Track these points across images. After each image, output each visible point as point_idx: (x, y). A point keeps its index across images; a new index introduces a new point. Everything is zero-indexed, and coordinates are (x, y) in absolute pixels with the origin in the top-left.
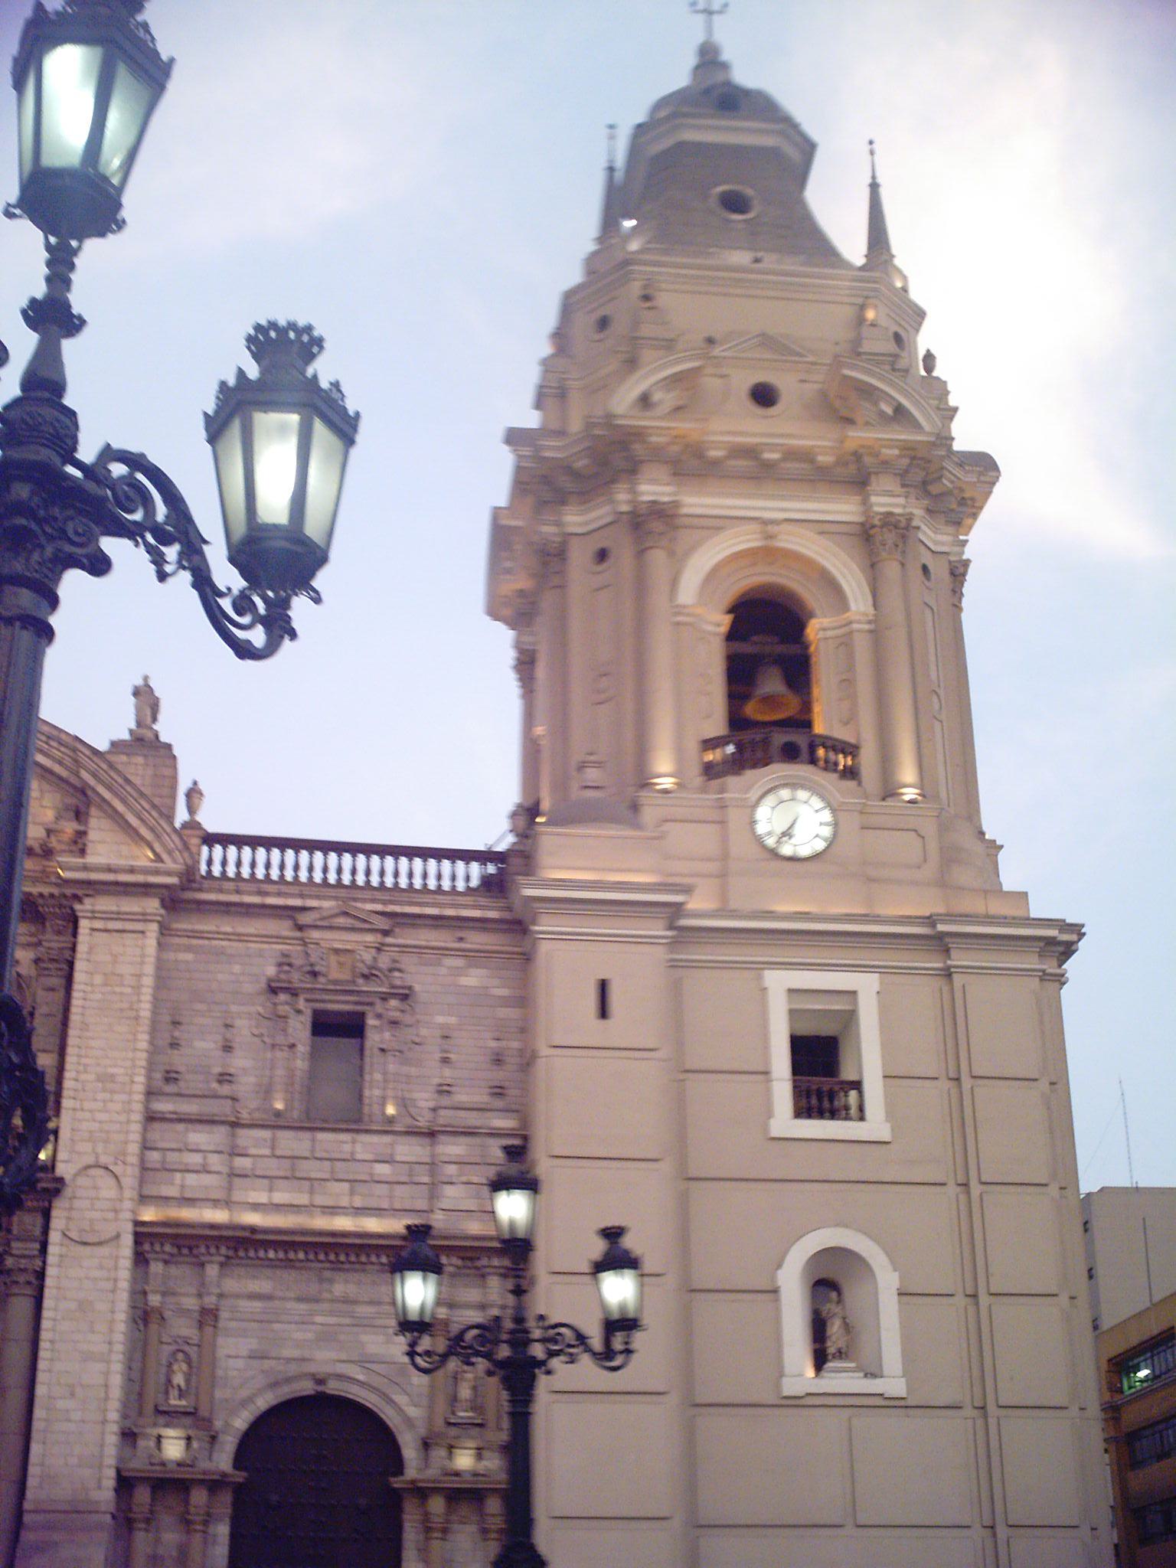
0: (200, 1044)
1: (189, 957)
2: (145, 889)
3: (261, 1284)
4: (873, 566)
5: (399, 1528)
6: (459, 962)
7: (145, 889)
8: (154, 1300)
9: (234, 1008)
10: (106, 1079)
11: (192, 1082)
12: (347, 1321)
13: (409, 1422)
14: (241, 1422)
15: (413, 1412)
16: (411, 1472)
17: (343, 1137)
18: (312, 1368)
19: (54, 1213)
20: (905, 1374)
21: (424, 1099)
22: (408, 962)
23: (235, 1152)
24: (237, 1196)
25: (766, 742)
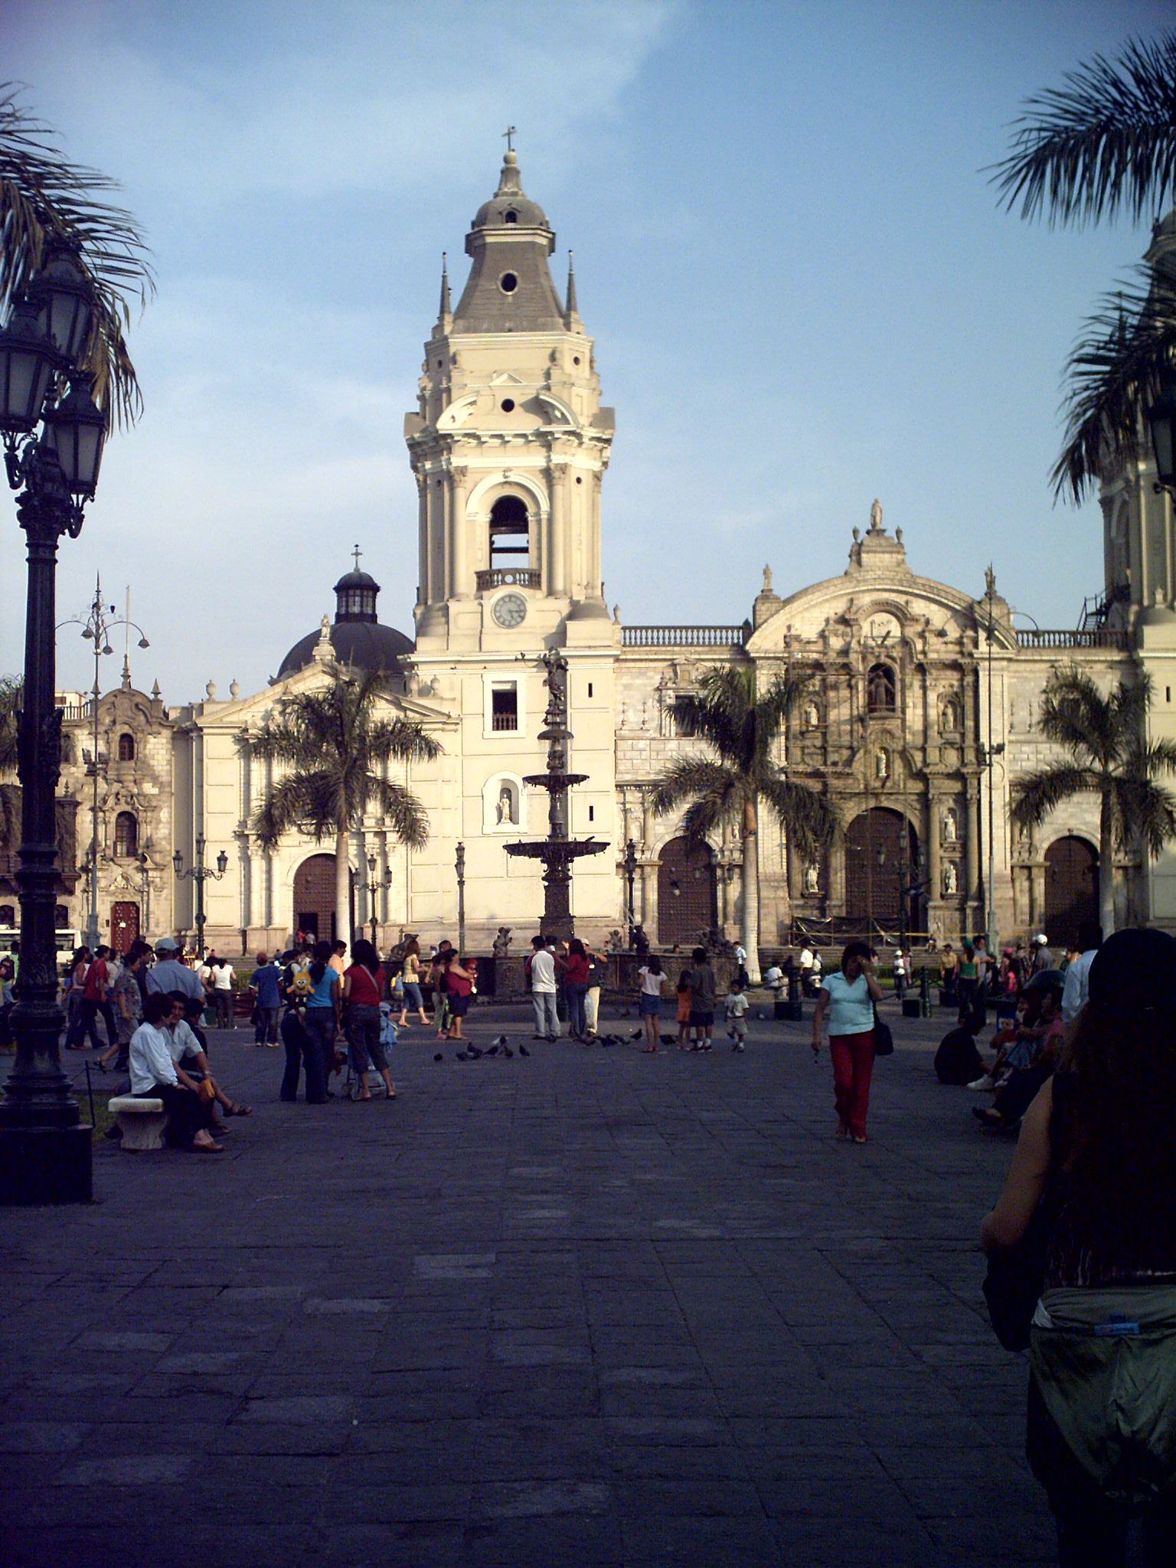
0: (1021, 713)
1: (1015, 680)
7: (1003, 659)
14: (1046, 845)
18: (1068, 827)
19: (982, 779)
23: (1037, 752)
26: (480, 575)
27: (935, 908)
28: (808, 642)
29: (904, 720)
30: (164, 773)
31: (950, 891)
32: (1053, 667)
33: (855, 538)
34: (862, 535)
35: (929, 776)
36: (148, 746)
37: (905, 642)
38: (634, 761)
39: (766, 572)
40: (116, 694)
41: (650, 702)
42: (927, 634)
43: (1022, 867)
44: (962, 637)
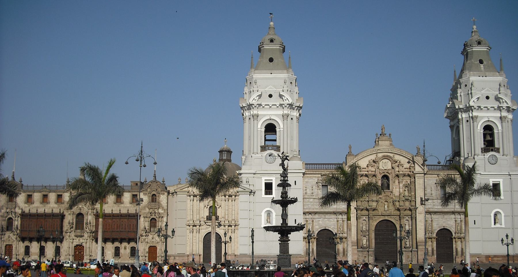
3: (437, 217)
4: (502, 123)
5: (453, 242)
9: (432, 186)
13: (453, 230)
16: (454, 236)
18: (443, 226)
19: (417, 211)
20: (505, 224)
25: (489, 149)
26: (262, 147)
30: (165, 206)
31: (407, 246)
32: (438, 176)
33: (377, 137)
34: (379, 136)
35: (401, 210)
36: (161, 198)
37: (393, 168)
38: (309, 205)
39: (350, 147)
40: (152, 182)
41: (314, 187)
42: (399, 166)
43: (429, 238)
44: (410, 167)
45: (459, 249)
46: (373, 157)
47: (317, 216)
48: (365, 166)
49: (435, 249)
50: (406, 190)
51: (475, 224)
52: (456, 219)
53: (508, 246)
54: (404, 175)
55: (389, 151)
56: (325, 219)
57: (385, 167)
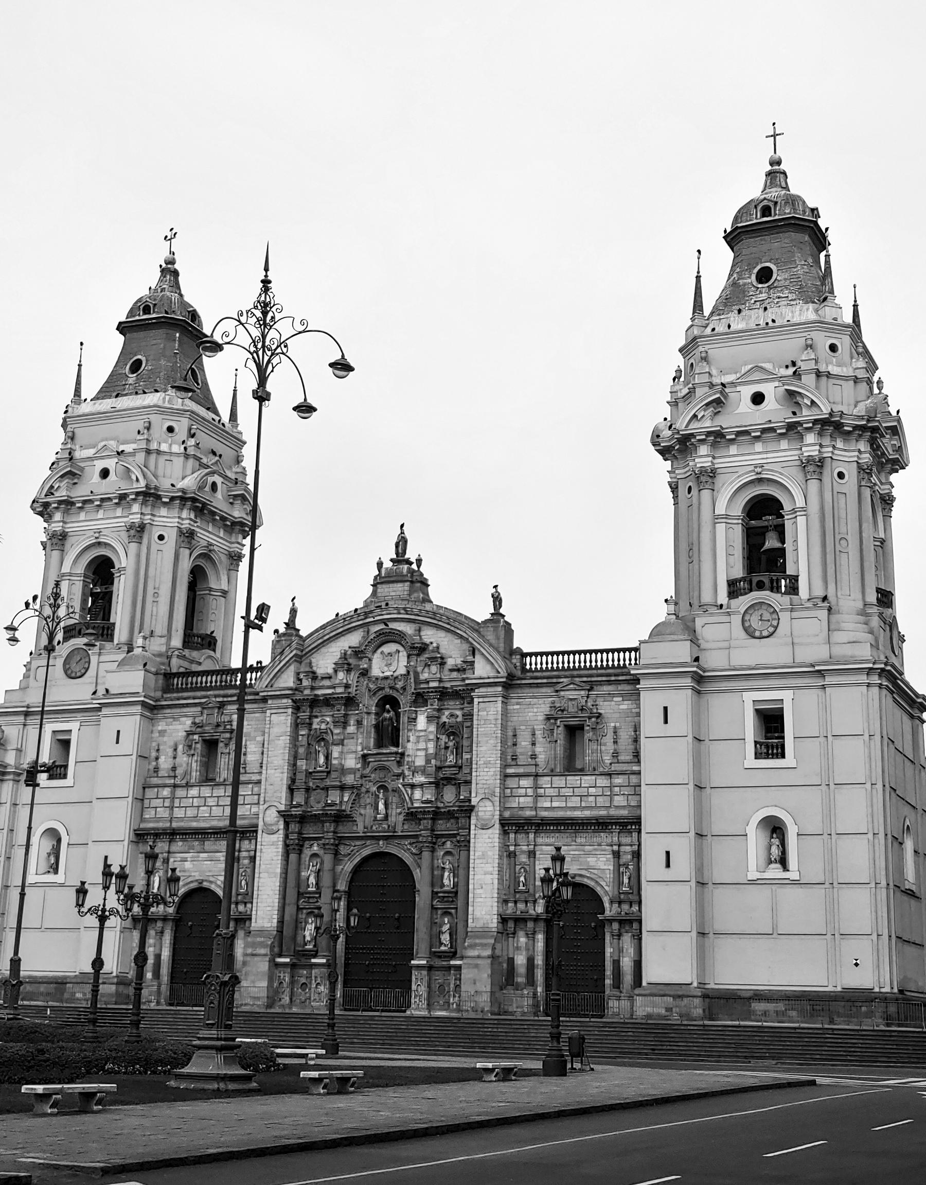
0: (523, 743)
1: (518, 707)
2: (495, 684)
6: (621, 699)
7: (495, 684)
8: (512, 848)
9: (535, 727)
10: (487, 763)
11: (522, 760)
12: (583, 853)
13: (606, 892)
15: (607, 888)
16: (607, 913)
17: (577, 778)
21: (607, 759)
22: (600, 702)
24: (539, 805)
27: (419, 967)
28: (323, 678)
29: (402, 755)
41: (180, 748)
45: (627, 963)
46: (354, 639)
47: (180, 843)
48: (330, 671)
49: (539, 960)
50: (451, 744)
51: (668, 865)
52: (615, 848)
53: (103, 919)
54: (444, 694)
55: (399, 613)
56: (202, 855)
57: (386, 668)
